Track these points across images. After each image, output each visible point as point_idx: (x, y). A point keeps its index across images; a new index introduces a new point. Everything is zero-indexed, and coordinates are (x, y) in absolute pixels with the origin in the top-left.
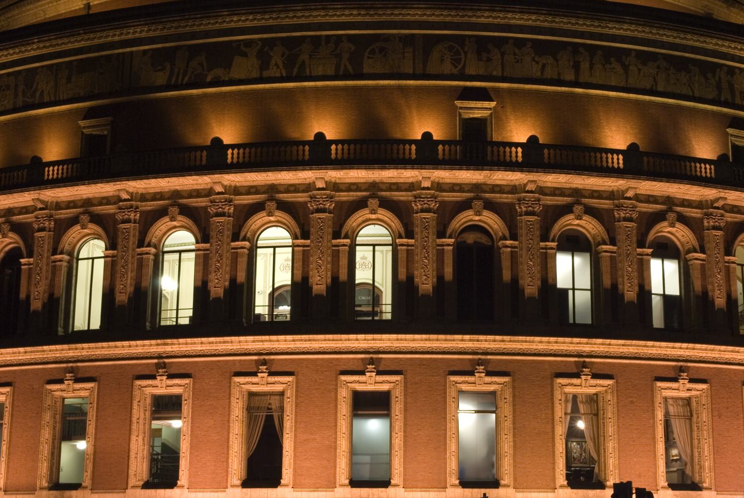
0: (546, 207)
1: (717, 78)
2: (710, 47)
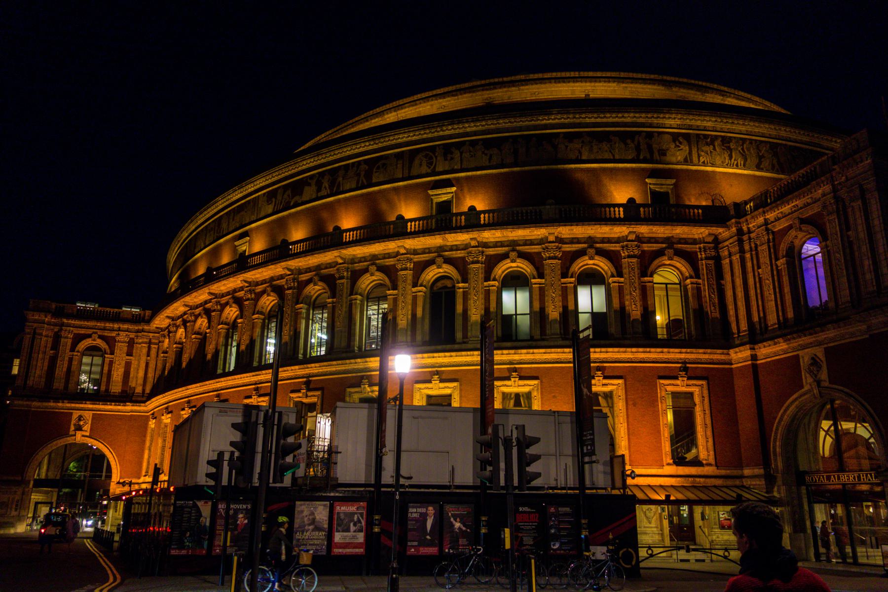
0: (489, 257)
1: (636, 142)
2: (629, 120)
